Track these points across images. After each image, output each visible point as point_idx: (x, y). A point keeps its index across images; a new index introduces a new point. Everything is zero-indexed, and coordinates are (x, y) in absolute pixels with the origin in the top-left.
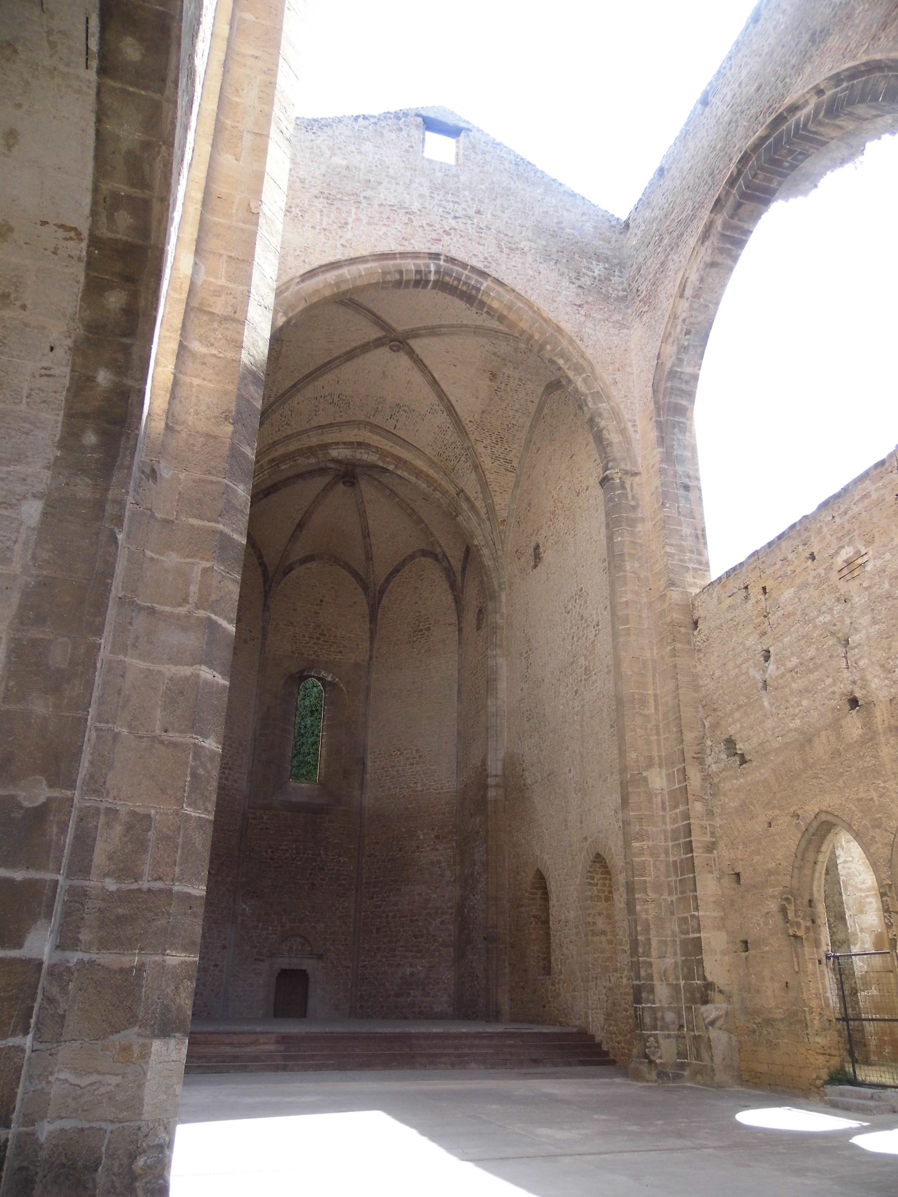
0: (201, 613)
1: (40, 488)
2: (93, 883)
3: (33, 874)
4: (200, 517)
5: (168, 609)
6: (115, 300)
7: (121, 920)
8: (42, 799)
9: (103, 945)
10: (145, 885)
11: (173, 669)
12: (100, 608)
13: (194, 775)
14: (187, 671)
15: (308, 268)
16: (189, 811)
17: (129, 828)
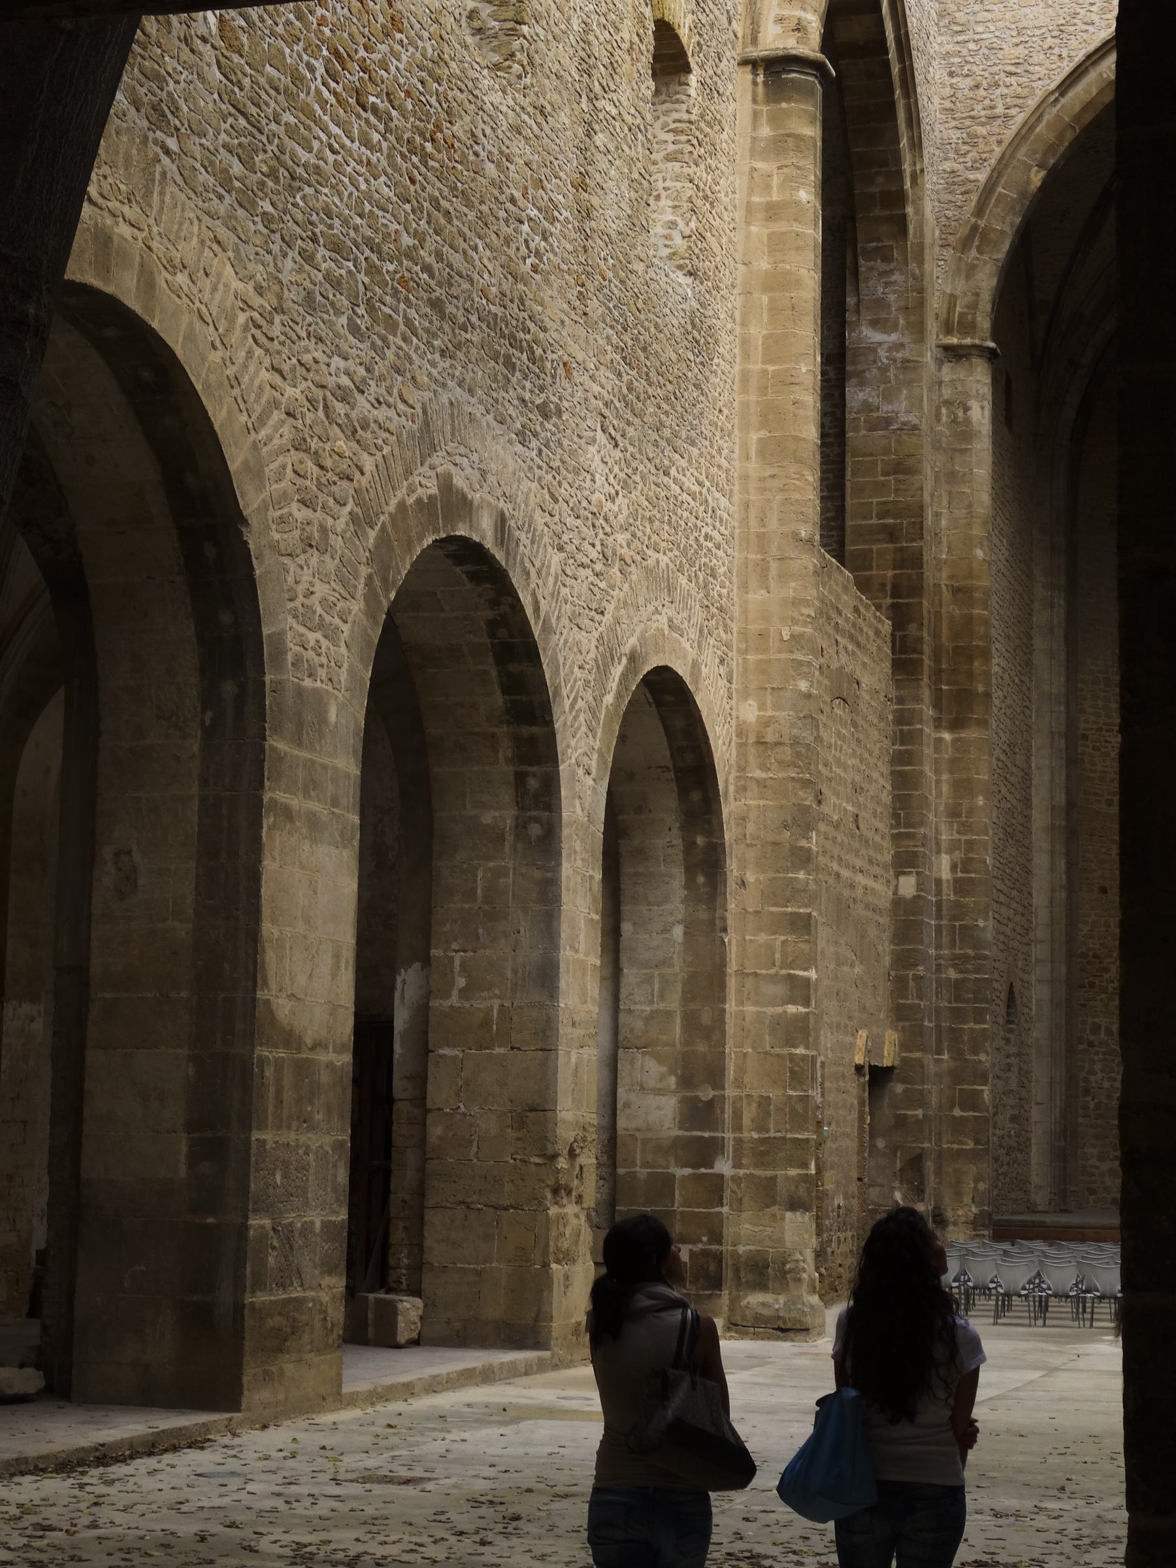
0: (784, 972)
1: (680, 917)
2: (746, 1135)
3: (712, 1134)
4: (776, 905)
5: (764, 972)
6: (696, 796)
7: (762, 1154)
8: (710, 1097)
9: (756, 1166)
10: (772, 1134)
11: (772, 1009)
12: (723, 986)
13: (792, 1071)
14: (780, 1010)
15: (1067, 67)
16: (791, 1093)
17: (760, 1105)
